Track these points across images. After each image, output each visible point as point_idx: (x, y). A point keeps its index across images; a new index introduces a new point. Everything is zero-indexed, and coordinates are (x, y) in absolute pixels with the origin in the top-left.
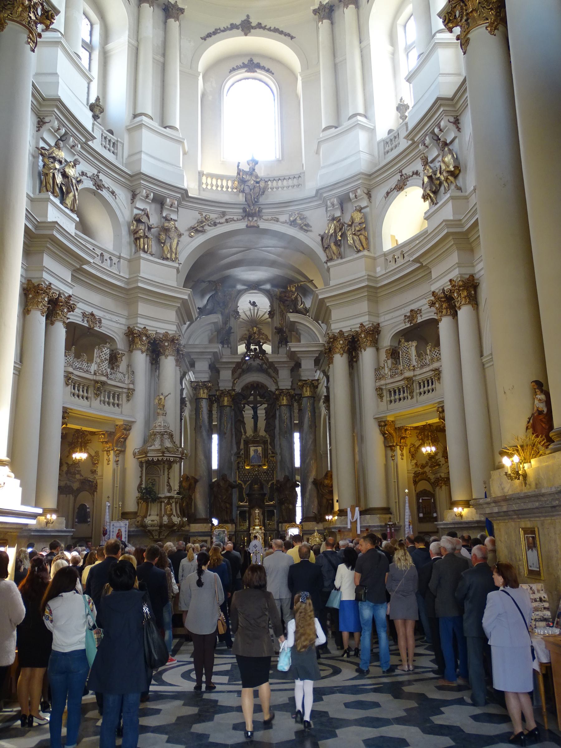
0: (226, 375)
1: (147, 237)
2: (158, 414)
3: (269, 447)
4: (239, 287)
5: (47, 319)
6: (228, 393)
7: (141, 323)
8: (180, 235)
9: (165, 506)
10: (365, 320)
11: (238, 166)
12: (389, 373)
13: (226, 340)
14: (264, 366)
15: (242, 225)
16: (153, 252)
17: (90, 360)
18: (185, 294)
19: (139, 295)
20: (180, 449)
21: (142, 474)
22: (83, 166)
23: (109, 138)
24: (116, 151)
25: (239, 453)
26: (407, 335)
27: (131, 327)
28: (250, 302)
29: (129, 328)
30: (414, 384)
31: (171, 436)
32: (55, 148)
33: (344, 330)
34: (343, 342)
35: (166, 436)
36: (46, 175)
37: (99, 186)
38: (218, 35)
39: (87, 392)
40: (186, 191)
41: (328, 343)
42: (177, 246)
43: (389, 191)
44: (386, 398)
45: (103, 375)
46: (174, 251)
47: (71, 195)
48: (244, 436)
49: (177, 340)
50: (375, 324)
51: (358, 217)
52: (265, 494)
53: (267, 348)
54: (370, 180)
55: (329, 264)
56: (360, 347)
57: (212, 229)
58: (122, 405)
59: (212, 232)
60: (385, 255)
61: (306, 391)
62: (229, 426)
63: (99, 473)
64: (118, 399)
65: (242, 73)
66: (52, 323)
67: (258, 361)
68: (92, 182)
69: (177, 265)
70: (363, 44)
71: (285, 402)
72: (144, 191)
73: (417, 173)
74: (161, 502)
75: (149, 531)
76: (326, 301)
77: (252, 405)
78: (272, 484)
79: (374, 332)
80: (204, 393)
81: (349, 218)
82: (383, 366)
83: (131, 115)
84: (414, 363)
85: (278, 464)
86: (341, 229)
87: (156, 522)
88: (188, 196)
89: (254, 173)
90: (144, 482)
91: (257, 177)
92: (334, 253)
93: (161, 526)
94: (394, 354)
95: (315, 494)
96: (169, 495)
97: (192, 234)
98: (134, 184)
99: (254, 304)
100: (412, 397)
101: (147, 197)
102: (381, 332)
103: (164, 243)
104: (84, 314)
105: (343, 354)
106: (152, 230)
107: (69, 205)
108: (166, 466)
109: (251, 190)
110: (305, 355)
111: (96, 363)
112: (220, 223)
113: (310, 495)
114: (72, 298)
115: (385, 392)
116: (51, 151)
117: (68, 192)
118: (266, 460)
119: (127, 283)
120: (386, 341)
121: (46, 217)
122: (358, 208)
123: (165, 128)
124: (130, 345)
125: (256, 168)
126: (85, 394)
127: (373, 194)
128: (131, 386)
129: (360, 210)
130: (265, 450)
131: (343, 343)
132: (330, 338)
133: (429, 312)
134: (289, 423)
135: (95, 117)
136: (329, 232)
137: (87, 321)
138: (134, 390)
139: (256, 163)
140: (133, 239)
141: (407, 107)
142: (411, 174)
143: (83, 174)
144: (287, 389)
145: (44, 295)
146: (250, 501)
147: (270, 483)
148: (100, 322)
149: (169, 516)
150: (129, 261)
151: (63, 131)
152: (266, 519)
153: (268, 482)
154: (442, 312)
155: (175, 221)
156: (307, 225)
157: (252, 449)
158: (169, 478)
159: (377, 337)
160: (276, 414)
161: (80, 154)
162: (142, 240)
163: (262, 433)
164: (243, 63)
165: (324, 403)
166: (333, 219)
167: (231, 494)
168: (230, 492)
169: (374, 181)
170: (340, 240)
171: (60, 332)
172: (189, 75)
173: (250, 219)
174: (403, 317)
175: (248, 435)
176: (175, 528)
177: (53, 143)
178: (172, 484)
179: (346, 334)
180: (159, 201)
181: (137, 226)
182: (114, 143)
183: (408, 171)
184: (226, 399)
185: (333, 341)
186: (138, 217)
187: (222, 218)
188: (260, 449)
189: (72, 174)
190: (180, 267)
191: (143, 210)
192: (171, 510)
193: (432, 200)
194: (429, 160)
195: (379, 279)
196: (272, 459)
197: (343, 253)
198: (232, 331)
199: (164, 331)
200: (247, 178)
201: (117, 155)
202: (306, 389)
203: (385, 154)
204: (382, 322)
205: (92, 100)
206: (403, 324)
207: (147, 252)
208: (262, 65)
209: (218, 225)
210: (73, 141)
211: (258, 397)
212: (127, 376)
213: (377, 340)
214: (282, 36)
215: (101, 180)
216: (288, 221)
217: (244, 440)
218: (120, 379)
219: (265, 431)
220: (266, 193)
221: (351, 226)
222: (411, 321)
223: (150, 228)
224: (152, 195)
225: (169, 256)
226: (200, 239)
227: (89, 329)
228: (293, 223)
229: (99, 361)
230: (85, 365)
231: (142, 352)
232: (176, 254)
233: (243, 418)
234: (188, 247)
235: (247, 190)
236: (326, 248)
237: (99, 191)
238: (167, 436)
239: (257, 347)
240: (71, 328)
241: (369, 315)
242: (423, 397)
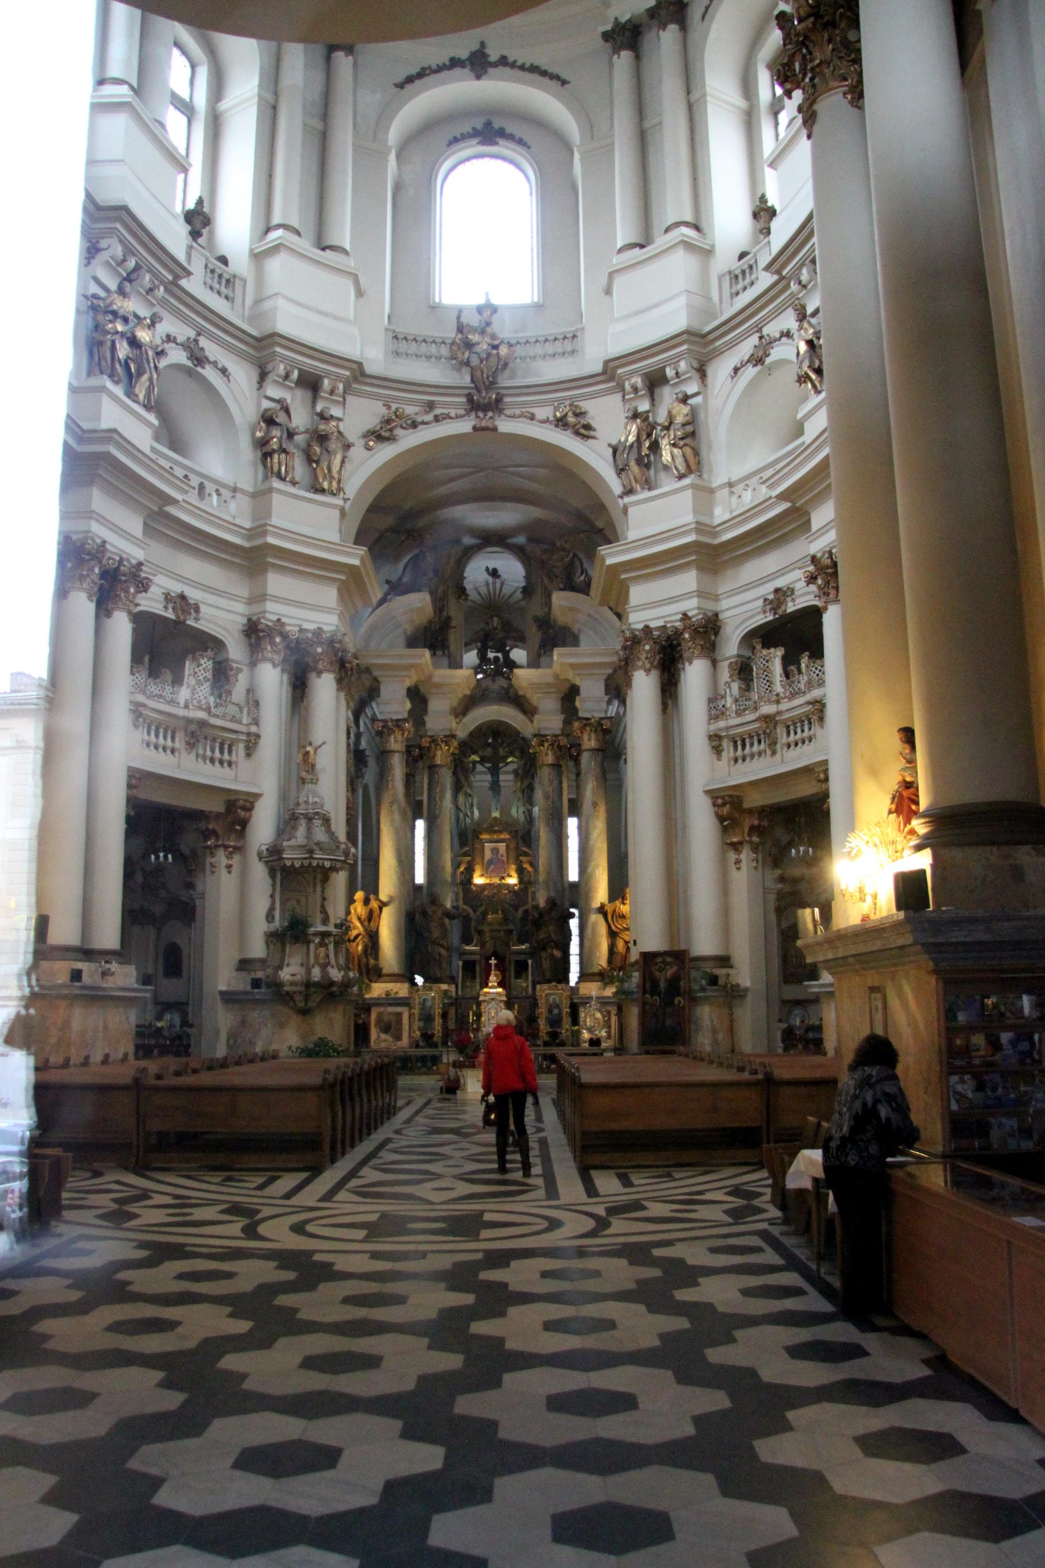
1: (284, 451)
2: (303, 781)
4: (468, 541)
5: (99, 605)
7: (273, 611)
8: (348, 446)
9: (316, 949)
10: (691, 605)
11: (458, 318)
12: (734, 707)
15: (464, 426)
16: (297, 479)
17: (178, 681)
18: (355, 557)
19: (270, 560)
20: (343, 846)
21: (274, 890)
22: (168, 325)
23: (218, 271)
24: (231, 294)
26: (765, 636)
27: (254, 618)
28: (487, 569)
29: (249, 620)
30: (778, 731)
31: (326, 821)
32: (116, 295)
33: (653, 624)
35: (317, 822)
36: (101, 343)
37: (199, 358)
38: (426, 80)
39: (173, 740)
40: (360, 365)
41: (625, 648)
42: (341, 466)
43: (739, 365)
44: (728, 751)
45: (200, 708)
46: (336, 476)
47: (145, 377)
49: (340, 642)
50: (710, 614)
51: (682, 413)
53: (518, 655)
54: (706, 345)
55: (627, 500)
56: (681, 656)
57: (408, 435)
58: (236, 763)
59: (409, 440)
60: (730, 485)
61: (589, 740)
63: (199, 887)
64: (230, 752)
65: (473, 147)
66: (109, 614)
67: (501, 682)
68: (184, 354)
69: (341, 503)
70: (695, 95)
71: (550, 759)
72: (282, 367)
73: (787, 334)
74: (308, 942)
75: (288, 993)
77: (488, 765)
79: (707, 631)
80: (396, 741)
81: (666, 413)
82: (723, 693)
83: (262, 227)
84: (778, 688)
86: (649, 435)
87: (298, 978)
88: (363, 374)
89: (489, 330)
90: (277, 906)
91: (493, 337)
92: (636, 480)
93: (308, 984)
94: (744, 671)
96: (322, 928)
97: (371, 443)
98: (265, 353)
100: (774, 753)
101: (287, 377)
102: (722, 631)
103: (317, 462)
104: (167, 597)
106: (297, 438)
107: (141, 397)
108: (319, 877)
109: (481, 361)
111: (189, 686)
112: (423, 423)
114: (143, 568)
115: (725, 743)
116: (108, 301)
117: (140, 373)
119: (249, 538)
120: (731, 646)
121: (98, 417)
122: (680, 396)
123: (323, 249)
124: (252, 653)
125: (495, 319)
126: (169, 743)
127: (710, 371)
128: (253, 729)
129: (685, 399)
132: (626, 640)
133: (804, 594)
135: (195, 234)
136: (627, 440)
137: (173, 609)
138: (258, 736)
139: (495, 310)
140: (259, 454)
141: (772, 213)
142: (778, 336)
143: (169, 339)
144: (555, 736)
145: (92, 563)
148: (197, 610)
149: (324, 967)
150: (254, 496)
151: (131, 263)
154: (828, 594)
155: (339, 419)
156: (588, 427)
157: (488, 846)
158: (324, 899)
159: (713, 637)
161: (163, 302)
162: (276, 456)
164: (474, 129)
166: (635, 416)
169: (711, 347)
170: (648, 456)
171: (121, 629)
172: (369, 151)
173: (481, 415)
174: (760, 602)
176: (334, 989)
177: (113, 285)
178: (330, 911)
179: (656, 633)
180: (310, 384)
181: (267, 432)
182: (228, 281)
183: (772, 329)
185: (632, 645)
186: (269, 413)
187: (427, 413)
188: (502, 846)
189: (148, 339)
191: (278, 401)
192: (327, 956)
193: (814, 386)
194: (810, 310)
195: (718, 529)
197: (653, 478)
198: (453, 623)
200: (474, 338)
201: (233, 302)
203: (732, 298)
204: (722, 611)
205: (191, 205)
206: (762, 616)
207: (283, 480)
208: (508, 131)
209: (421, 427)
210: (151, 280)
212: (245, 710)
214: (546, 81)
215: (202, 349)
216: (551, 418)
218: (234, 717)
220: (511, 365)
221: (667, 428)
222: (774, 610)
223: (291, 435)
224: (295, 374)
225: (326, 485)
226: (386, 453)
227: (179, 623)
228: (561, 423)
229: (193, 682)
230: (168, 689)
231: (275, 666)
232: (339, 482)
234: (362, 469)
235: (475, 361)
236: (620, 471)
237: (199, 369)
238: (320, 822)
239: (500, 655)
240: (143, 622)
241: (698, 596)
242: (793, 753)
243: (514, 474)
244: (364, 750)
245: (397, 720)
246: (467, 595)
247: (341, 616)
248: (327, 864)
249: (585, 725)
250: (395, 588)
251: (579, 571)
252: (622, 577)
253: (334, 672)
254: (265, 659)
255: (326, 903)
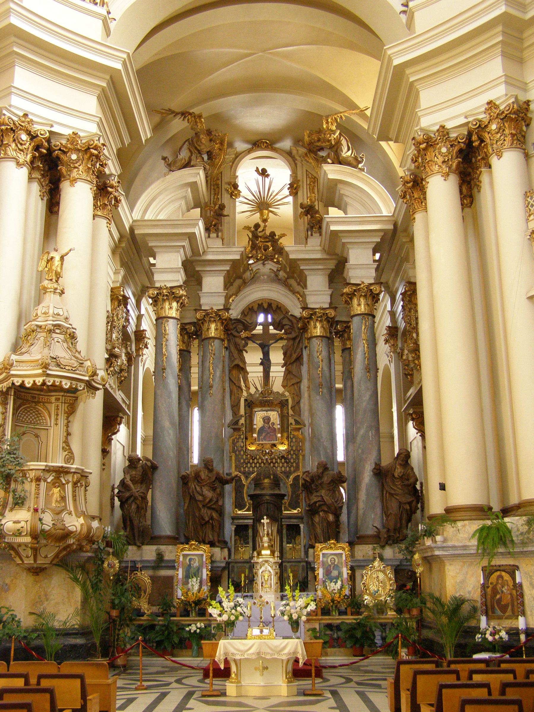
0: (213, 285)
3: (291, 412)
6: (217, 313)
9: (48, 489)
13: (215, 226)
14: (282, 274)
25: (237, 423)
28: (257, 170)
34: (448, 150)
48: (245, 394)
52: (283, 496)
61: (359, 305)
62: (218, 374)
67: (270, 266)
76: (408, 71)
77: (258, 342)
78: (296, 479)
85: (307, 445)
95: (377, 493)
99: (263, 173)
105: (448, 175)
110: (356, 241)
113: (368, 494)
118: (285, 435)
130: (283, 417)
131: (448, 152)
134: (326, 369)
146: (256, 508)
147: (292, 477)
152: (285, 540)
153: (288, 474)
158: (69, 434)
160: (302, 354)
163: (277, 386)
165: (386, 341)
167: (222, 495)
168: (218, 490)
175: (252, 390)
176: (71, 541)
178: (75, 447)
179: (453, 135)
184: (213, 326)
190: (112, 25)
192: (63, 498)
196: (296, 433)
198: (225, 212)
199: (70, 132)
202: (359, 300)
211: (271, 327)
213: (524, 137)
217: (246, 400)
219: (284, 386)
231: (18, 164)
233: (244, 363)
238: (62, 337)
243: (287, 56)
244: (144, 330)
245: (172, 288)
246: (240, 192)
247: (100, 125)
248: (66, 384)
249: (355, 291)
250: (172, 166)
251: (346, 148)
252: (411, 80)
253: (91, 182)
254: (7, 158)
255: (69, 437)
